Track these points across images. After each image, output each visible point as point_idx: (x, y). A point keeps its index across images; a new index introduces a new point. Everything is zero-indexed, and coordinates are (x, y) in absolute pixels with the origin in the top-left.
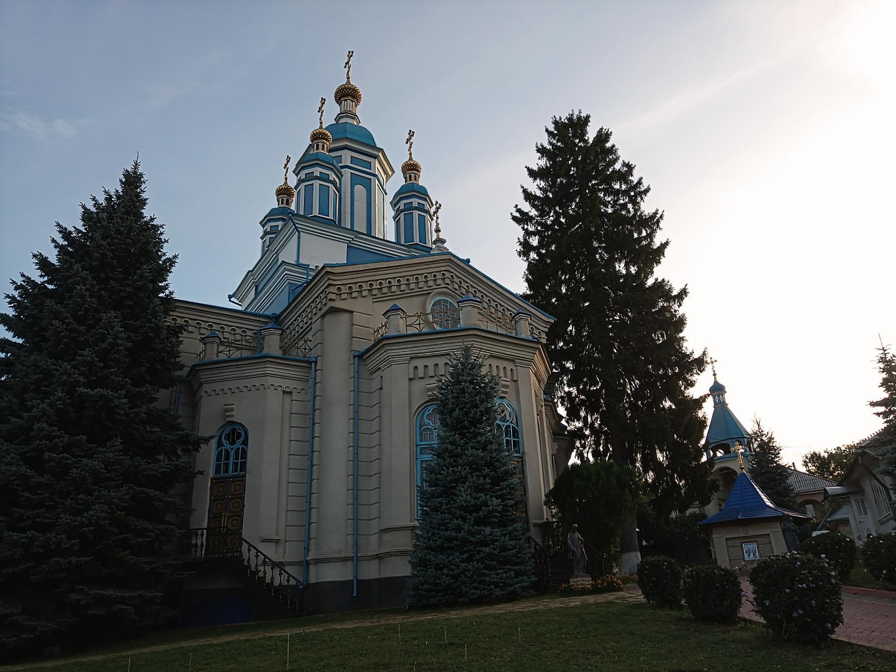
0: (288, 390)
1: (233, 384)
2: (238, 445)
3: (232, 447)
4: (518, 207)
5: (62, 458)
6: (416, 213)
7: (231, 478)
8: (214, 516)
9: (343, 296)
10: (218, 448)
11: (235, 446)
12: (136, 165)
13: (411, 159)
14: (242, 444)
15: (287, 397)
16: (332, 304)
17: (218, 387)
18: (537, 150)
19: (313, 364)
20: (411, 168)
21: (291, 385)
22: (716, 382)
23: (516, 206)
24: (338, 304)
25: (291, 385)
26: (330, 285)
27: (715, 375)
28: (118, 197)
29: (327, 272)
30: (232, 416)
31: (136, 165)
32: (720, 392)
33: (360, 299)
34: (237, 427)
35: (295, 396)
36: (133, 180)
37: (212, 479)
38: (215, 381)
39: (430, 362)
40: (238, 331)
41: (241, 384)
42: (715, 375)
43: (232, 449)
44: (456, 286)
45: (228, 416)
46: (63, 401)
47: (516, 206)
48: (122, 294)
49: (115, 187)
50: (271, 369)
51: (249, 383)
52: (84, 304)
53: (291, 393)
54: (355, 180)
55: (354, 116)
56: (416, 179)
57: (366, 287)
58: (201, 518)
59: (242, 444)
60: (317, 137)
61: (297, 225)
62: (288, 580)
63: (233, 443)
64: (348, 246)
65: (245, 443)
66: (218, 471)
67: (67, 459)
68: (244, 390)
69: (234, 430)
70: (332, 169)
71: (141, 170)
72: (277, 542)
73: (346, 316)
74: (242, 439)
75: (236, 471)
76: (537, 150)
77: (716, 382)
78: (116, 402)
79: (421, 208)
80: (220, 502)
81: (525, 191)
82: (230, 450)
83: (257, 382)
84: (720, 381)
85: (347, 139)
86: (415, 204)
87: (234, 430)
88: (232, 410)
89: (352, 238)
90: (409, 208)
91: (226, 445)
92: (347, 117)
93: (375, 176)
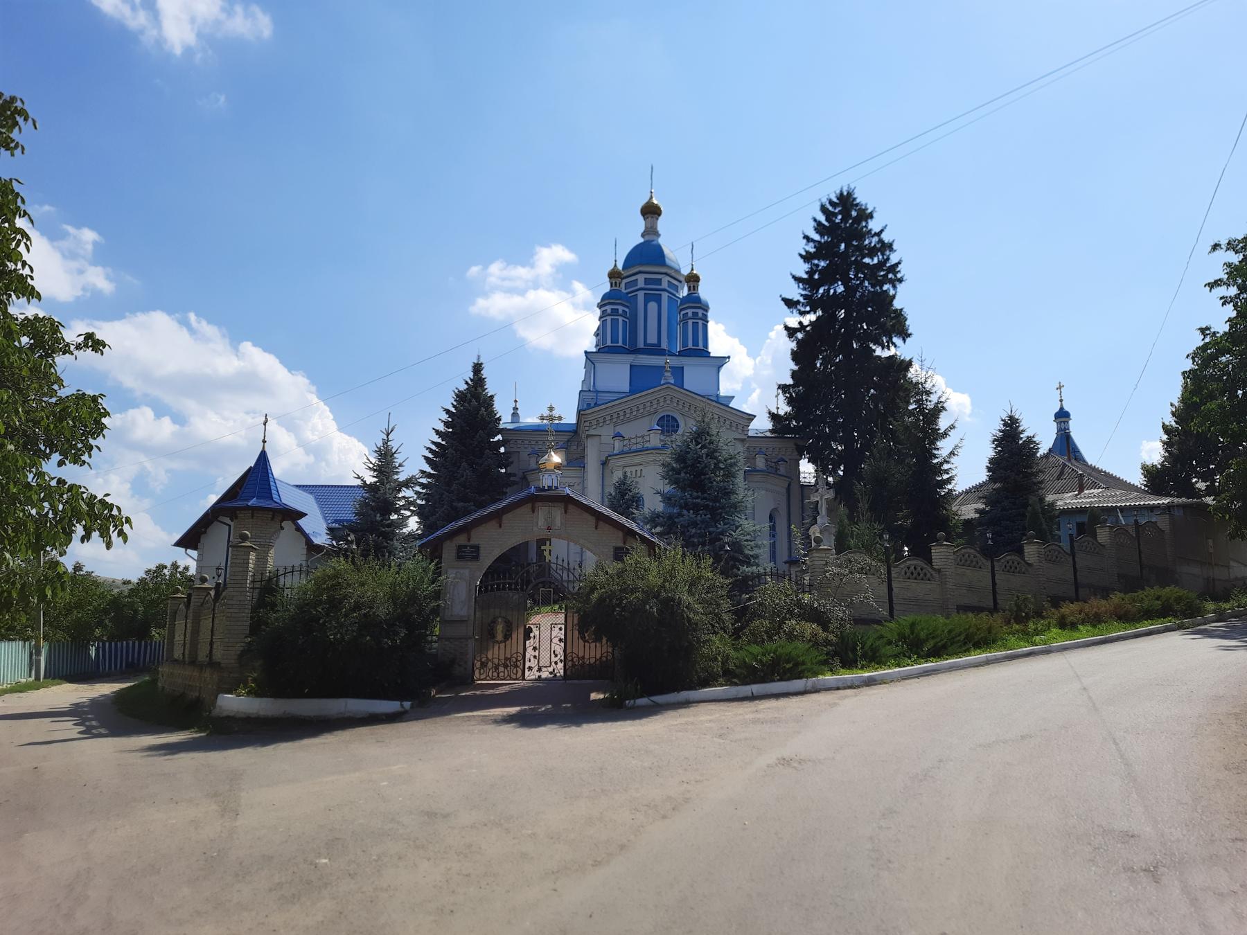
6: (690, 322)
16: (587, 433)
20: (693, 279)
22: (1062, 408)
24: (592, 432)
27: (1061, 401)
28: (471, 380)
32: (1066, 419)
36: (477, 368)
39: (633, 469)
42: (1061, 401)
47: (781, 296)
54: (648, 299)
57: (608, 418)
71: (481, 360)
73: (598, 438)
77: (1062, 408)
81: (794, 278)
84: (1066, 408)
90: (685, 319)
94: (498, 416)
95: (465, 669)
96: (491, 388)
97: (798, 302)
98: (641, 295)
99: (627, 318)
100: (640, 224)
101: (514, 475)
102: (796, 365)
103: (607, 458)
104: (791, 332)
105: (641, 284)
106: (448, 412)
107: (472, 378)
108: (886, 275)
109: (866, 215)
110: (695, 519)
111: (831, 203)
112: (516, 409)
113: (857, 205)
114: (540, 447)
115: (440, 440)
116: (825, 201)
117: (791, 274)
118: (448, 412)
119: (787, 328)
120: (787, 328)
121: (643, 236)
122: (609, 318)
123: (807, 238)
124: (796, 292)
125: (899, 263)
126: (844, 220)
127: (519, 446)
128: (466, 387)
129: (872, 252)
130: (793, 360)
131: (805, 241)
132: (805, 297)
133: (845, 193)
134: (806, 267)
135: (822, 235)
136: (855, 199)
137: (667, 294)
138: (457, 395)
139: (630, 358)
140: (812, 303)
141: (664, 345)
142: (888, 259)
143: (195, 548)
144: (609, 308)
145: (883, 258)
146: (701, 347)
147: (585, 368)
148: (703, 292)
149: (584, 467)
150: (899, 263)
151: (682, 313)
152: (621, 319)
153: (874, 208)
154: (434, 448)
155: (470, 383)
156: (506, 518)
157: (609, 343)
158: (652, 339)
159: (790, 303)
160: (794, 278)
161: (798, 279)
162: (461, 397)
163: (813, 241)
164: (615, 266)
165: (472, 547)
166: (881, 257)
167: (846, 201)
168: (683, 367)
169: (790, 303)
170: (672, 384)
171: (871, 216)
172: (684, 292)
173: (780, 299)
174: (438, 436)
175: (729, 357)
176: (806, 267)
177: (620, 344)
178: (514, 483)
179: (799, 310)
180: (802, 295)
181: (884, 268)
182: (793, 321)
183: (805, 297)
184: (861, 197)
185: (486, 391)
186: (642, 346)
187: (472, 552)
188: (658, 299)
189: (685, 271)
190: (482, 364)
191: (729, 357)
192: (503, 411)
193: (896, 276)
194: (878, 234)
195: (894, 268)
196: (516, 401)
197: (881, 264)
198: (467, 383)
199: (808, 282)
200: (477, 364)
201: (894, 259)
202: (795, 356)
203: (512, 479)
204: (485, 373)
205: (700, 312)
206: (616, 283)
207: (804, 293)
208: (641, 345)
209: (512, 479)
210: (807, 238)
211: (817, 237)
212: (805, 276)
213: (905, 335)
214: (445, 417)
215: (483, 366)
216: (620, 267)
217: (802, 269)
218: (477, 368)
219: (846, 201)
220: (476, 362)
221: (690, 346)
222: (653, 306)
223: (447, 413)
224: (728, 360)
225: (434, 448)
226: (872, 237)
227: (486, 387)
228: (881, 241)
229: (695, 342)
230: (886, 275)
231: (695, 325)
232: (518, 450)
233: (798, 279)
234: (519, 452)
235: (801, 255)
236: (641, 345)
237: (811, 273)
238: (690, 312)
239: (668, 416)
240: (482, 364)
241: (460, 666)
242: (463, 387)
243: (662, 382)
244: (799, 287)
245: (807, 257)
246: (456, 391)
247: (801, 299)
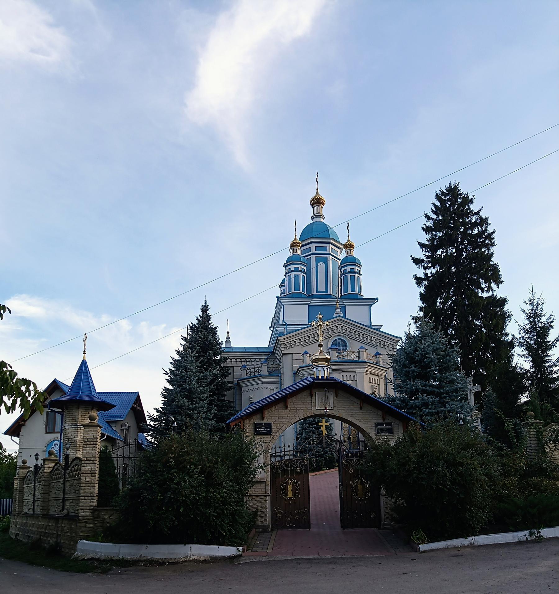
0: (272, 388)
1: (252, 387)
4: (413, 257)
9: (287, 348)
13: (348, 240)
16: (283, 352)
17: (247, 388)
18: (425, 216)
20: (349, 246)
21: (273, 386)
23: (411, 256)
25: (273, 386)
26: (281, 344)
33: (296, 347)
36: (205, 309)
38: (246, 386)
41: (254, 387)
44: (344, 331)
45: (251, 401)
47: (411, 256)
49: (199, 313)
50: (265, 381)
51: (257, 386)
53: (273, 389)
54: (318, 260)
55: (321, 216)
56: (350, 253)
60: (294, 245)
61: (281, 302)
64: (309, 306)
68: (256, 389)
70: (300, 264)
71: (207, 304)
73: (290, 355)
76: (425, 216)
79: (352, 271)
81: (419, 243)
83: (260, 386)
85: (312, 238)
86: (349, 270)
88: (252, 398)
89: (310, 302)
90: (346, 273)
92: (316, 217)
93: (330, 254)
94: (220, 341)
95: (266, 520)
96: (214, 322)
97: (423, 260)
98: (313, 257)
99: (305, 274)
100: (310, 211)
102: (423, 303)
103: (298, 369)
104: (419, 281)
105: (313, 250)
107: (201, 315)
108: (484, 241)
109: (467, 201)
110: (427, 401)
111: (443, 193)
112: (228, 338)
113: (461, 194)
114: (248, 363)
116: (439, 192)
117: (418, 241)
119: (416, 278)
120: (416, 278)
121: (312, 219)
122: (293, 274)
123: (427, 217)
124: (421, 254)
125: (494, 232)
126: (453, 204)
128: (197, 322)
129: (475, 225)
130: (421, 299)
131: (426, 219)
132: (428, 257)
133: (453, 187)
134: (428, 236)
135: (437, 215)
136: (459, 190)
137: (331, 257)
138: (191, 328)
139: (309, 301)
140: (434, 262)
141: (331, 292)
142: (486, 230)
144: (292, 267)
145: (482, 229)
146: (357, 292)
147: (275, 309)
148: (356, 254)
149: (281, 376)
150: (494, 232)
151: (343, 269)
152: (301, 274)
153: (474, 196)
155: (200, 318)
156: (291, 403)
157: (293, 291)
158: (322, 288)
159: (417, 261)
160: (419, 243)
161: (422, 245)
162: (194, 329)
163: (432, 219)
164: (295, 238)
165: (266, 424)
166: (480, 229)
167: (453, 191)
168: (345, 307)
169: (417, 261)
170: (341, 317)
171: (472, 202)
172: (343, 256)
173: (411, 258)
175: (377, 299)
176: (428, 236)
177: (301, 291)
178: (231, 388)
179: (424, 266)
180: (426, 255)
181: (483, 236)
182: (421, 273)
183: (428, 257)
184: (464, 189)
185: (211, 325)
186: (315, 293)
187: (266, 428)
188: (325, 261)
189: (343, 241)
190: (208, 306)
191: (377, 299)
192: (221, 336)
193: (491, 242)
194: (477, 213)
195: (490, 237)
196: (228, 333)
197: (480, 235)
198: (198, 319)
199: (431, 247)
200: (205, 306)
201: (490, 229)
202: (423, 297)
204: (210, 312)
205: (356, 268)
206: (296, 250)
207: (427, 254)
208: (314, 292)
209: (230, 385)
210: (427, 217)
211: (434, 217)
212: (427, 243)
213: (499, 282)
215: (209, 307)
216: (298, 237)
217: (425, 238)
218: (205, 309)
219: (453, 191)
220: (204, 305)
221: (349, 292)
222: (321, 265)
224: (376, 301)
226: (473, 215)
227: (210, 322)
228: (481, 218)
229: (353, 289)
230: (484, 241)
231: (353, 278)
233: (422, 245)
234: (233, 367)
235: (423, 228)
236: (314, 292)
237: (431, 240)
238: (349, 268)
239: (339, 339)
240: (208, 306)
241: (262, 517)
242: (195, 322)
243: (335, 315)
244: (423, 250)
245: (427, 230)
246: (191, 325)
247: (425, 258)
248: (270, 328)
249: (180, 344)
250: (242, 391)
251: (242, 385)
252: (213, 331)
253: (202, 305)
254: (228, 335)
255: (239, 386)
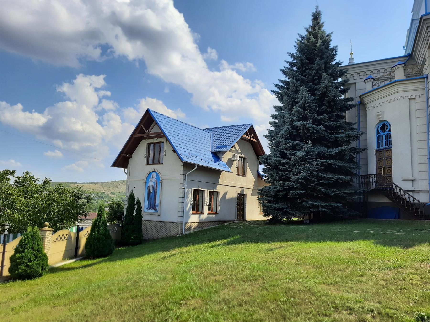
0: (412, 97)
1: (380, 101)
2: (387, 132)
3: (384, 133)
5: (290, 152)
7: (385, 149)
8: (379, 168)
10: (377, 135)
11: (386, 133)
12: (317, 7)
14: (389, 131)
15: (413, 102)
17: (373, 104)
19: (426, 79)
29: (424, 20)
30: (381, 118)
31: (317, 7)
34: (385, 123)
35: (418, 99)
36: (316, 17)
37: (376, 150)
40: (382, 71)
41: (384, 100)
43: (384, 134)
45: (379, 118)
46: (288, 129)
48: (312, 75)
52: (294, 85)
53: (414, 98)
58: (372, 169)
59: (389, 131)
62: (414, 201)
63: (384, 131)
65: (390, 131)
66: (378, 146)
67: (292, 152)
69: (384, 124)
72: (413, 180)
74: (388, 129)
75: (387, 145)
78: (308, 126)
80: (389, 160)
82: (383, 135)
87: (384, 124)
91: (382, 133)
96: (327, 29)
101: (351, 99)
106: (292, 55)
115: (287, 79)
118: (292, 55)
127: (355, 78)
128: (306, 33)
143: (127, 167)
154: (281, 84)
174: (285, 76)
178: (352, 106)
198: (307, 30)
203: (350, 103)
204: (322, 20)
214: (290, 59)
218: (316, 17)
223: (292, 57)
225: (281, 84)
232: (354, 81)
234: (355, 83)
248: (404, 47)
249: (285, 61)
250: (367, 109)
251: (366, 100)
252: (326, 42)
253: (313, 13)
254: (352, 57)
255: (362, 104)
